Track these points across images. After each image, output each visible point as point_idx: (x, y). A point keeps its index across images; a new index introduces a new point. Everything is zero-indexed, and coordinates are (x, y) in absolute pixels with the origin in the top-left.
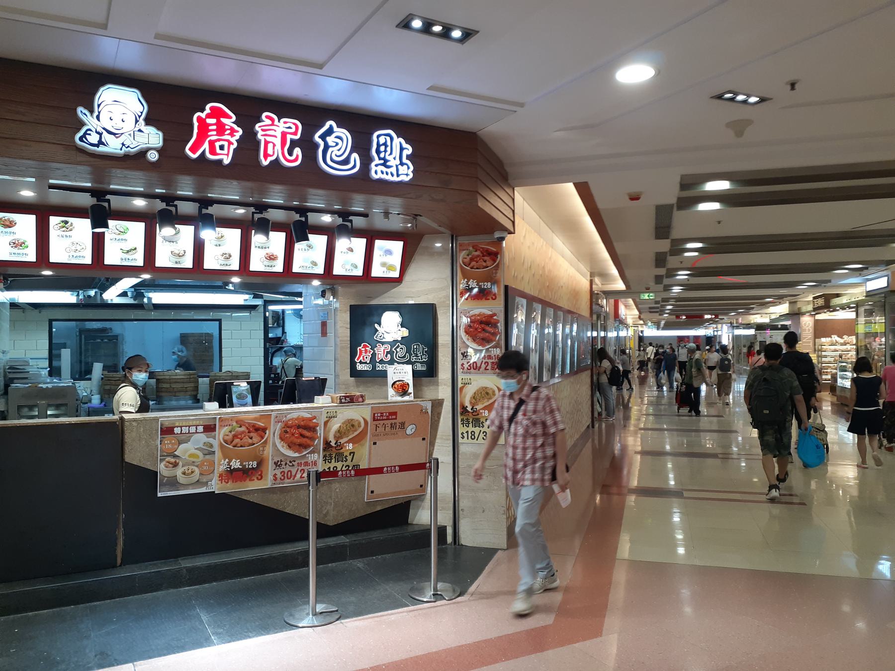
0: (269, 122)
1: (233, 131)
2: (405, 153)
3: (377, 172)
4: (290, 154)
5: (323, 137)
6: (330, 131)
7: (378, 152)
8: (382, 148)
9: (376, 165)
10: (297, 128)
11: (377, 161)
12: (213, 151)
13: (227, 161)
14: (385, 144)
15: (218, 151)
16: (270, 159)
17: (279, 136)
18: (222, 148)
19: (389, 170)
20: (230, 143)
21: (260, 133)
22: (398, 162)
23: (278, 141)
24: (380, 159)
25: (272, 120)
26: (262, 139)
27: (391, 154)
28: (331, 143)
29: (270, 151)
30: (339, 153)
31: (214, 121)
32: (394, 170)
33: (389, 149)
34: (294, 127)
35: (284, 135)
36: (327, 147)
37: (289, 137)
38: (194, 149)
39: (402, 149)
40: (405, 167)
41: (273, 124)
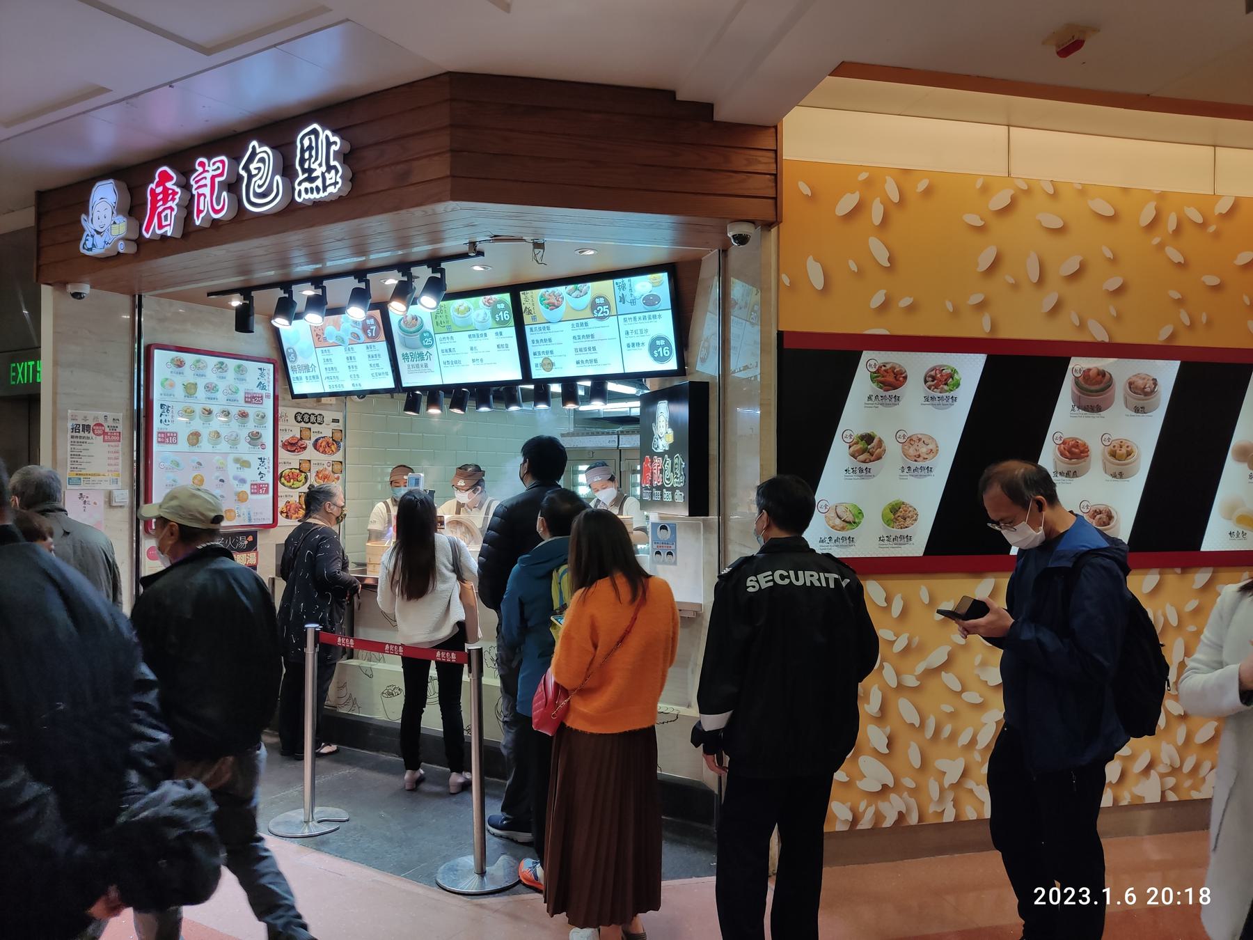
0: (200, 169)
1: (175, 193)
2: (334, 148)
3: (304, 193)
4: (218, 204)
5: (246, 168)
6: (254, 154)
7: (302, 161)
8: (307, 155)
9: (300, 184)
10: (222, 162)
11: (301, 177)
12: (161, 227)
13: (169, 231)
14: (310, 148)
15: (164, 223)
16: (202, 215)
17: (208, 182)
18: (166, 216)
19: (314, 185)
20: (171, 209)
21: (195, 186)
22: (324, 168)
23: (207, 191)
24: (304, 171)
25: (202, 164)
26: (195, 192)
27: (316, 159)
28: (254, 172)
29: (201, 208)
30: (260, 182)
31: (159, 190)
32: (319, 183)
33: (314, 153)
34: (220, 165)
35: (213, 178)
36: (250, 176)
37: (217, 180)
38: (147, 230)
39: (329, 144)
40: (333, 172)
41: (205, 171)
